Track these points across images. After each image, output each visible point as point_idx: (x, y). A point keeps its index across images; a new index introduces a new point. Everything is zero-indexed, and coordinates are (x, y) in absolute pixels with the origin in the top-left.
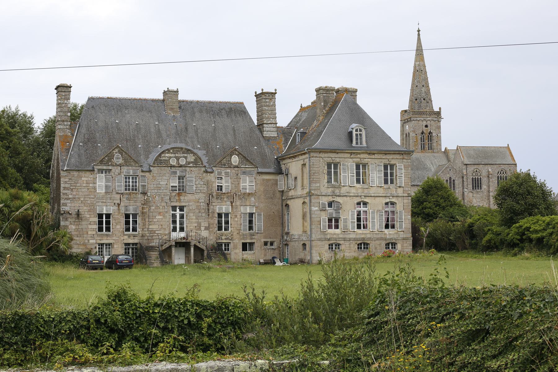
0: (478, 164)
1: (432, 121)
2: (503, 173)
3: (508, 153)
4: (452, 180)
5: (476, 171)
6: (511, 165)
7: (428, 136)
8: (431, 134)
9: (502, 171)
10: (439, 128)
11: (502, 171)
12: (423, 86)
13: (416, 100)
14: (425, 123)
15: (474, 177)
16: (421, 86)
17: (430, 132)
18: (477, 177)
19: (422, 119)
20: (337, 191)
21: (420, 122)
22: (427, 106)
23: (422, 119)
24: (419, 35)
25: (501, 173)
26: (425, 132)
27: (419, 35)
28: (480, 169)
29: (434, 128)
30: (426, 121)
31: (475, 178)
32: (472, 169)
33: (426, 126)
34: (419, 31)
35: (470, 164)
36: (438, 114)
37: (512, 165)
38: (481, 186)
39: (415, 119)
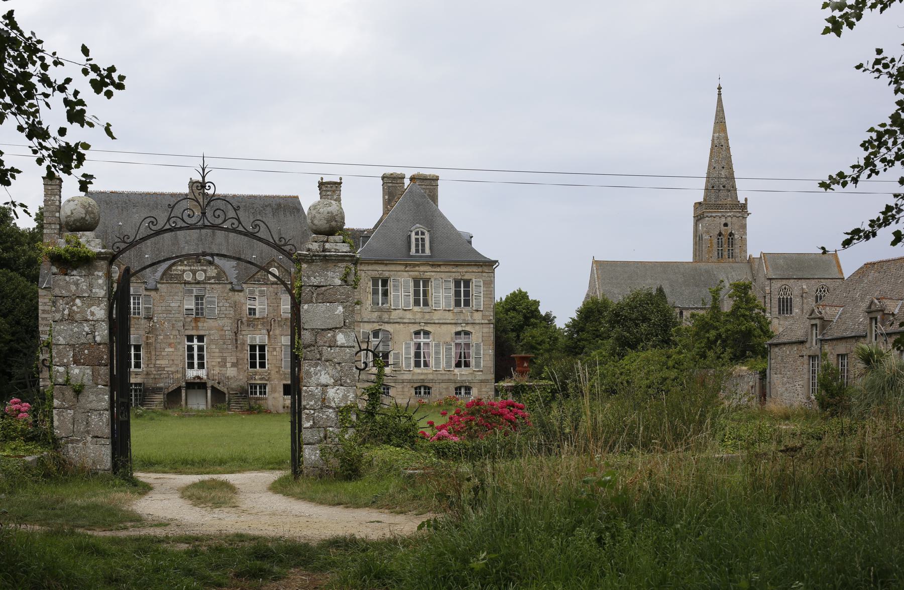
0: (787, 279)
1: (734, 218)
2: (824, 291)
3: (834, 262)
5: (785, 288)
6: (836, 280)
7: (729, 239)
8: (732, 237)
9: (823, 288)
10: (744, 227)
11: (823, 288)
12: (723, 168)
14: (723, 220)
15: (781, 297)
16: (720, 168)
17: (731, 232)
18: (785, 297)
19: (719, 214)
20: (385, 317)
21: (717, 219)
22: (728, 196)
23: (719, 214)
24: (720, 94)
25: (820, 291)
26: (723, 233)
27: (720, 94)
28: (790, 285)
29: (736, 227)
31: (783, 298)
32: (779, 285)
33: (726, 225)
34: (720, 88)
35: (777, 279)
37: (838, 280)
38: (791, 310)
39: (709, 215)
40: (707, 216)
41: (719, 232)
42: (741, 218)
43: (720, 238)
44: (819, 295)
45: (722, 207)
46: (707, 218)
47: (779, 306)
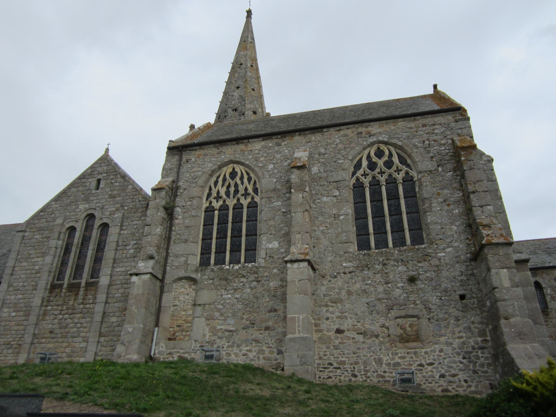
0: (238, 140)
2: (389, 164)
9: (380, 154)
15: (217, 205)
18: (231, 203)
25: (372, 166)
31: (224, 208)
44: (366, 181)
47: (207, 237)
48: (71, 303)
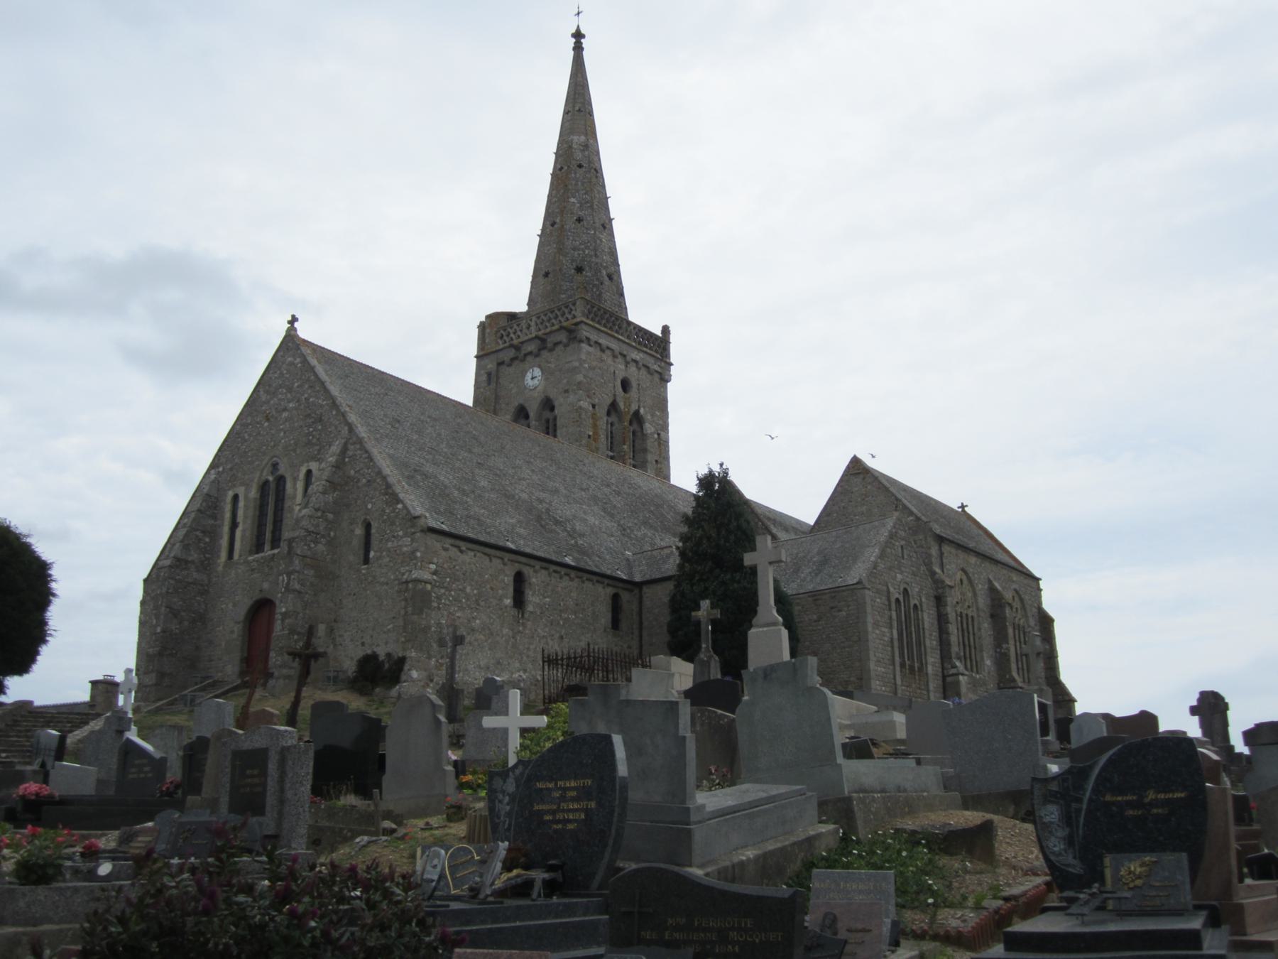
1: (643, 371)
4: (913, 602)
13: (579, 270)
14: (620, 370)
16: (598, 225)
17: (637, 413)
24: (578, 48)
26: (622, 405)
27: (578, 48)
28: (970, 570)
30: (627, 363)
34: (578, 35)
36: (658, 345)
39: (594, 337)
40: (588, 339)
41: (609, 401)
42: (656, 377)
43: (610, 420)
45: (620, 328)
46: (584, 345)
48: (914, 686)
